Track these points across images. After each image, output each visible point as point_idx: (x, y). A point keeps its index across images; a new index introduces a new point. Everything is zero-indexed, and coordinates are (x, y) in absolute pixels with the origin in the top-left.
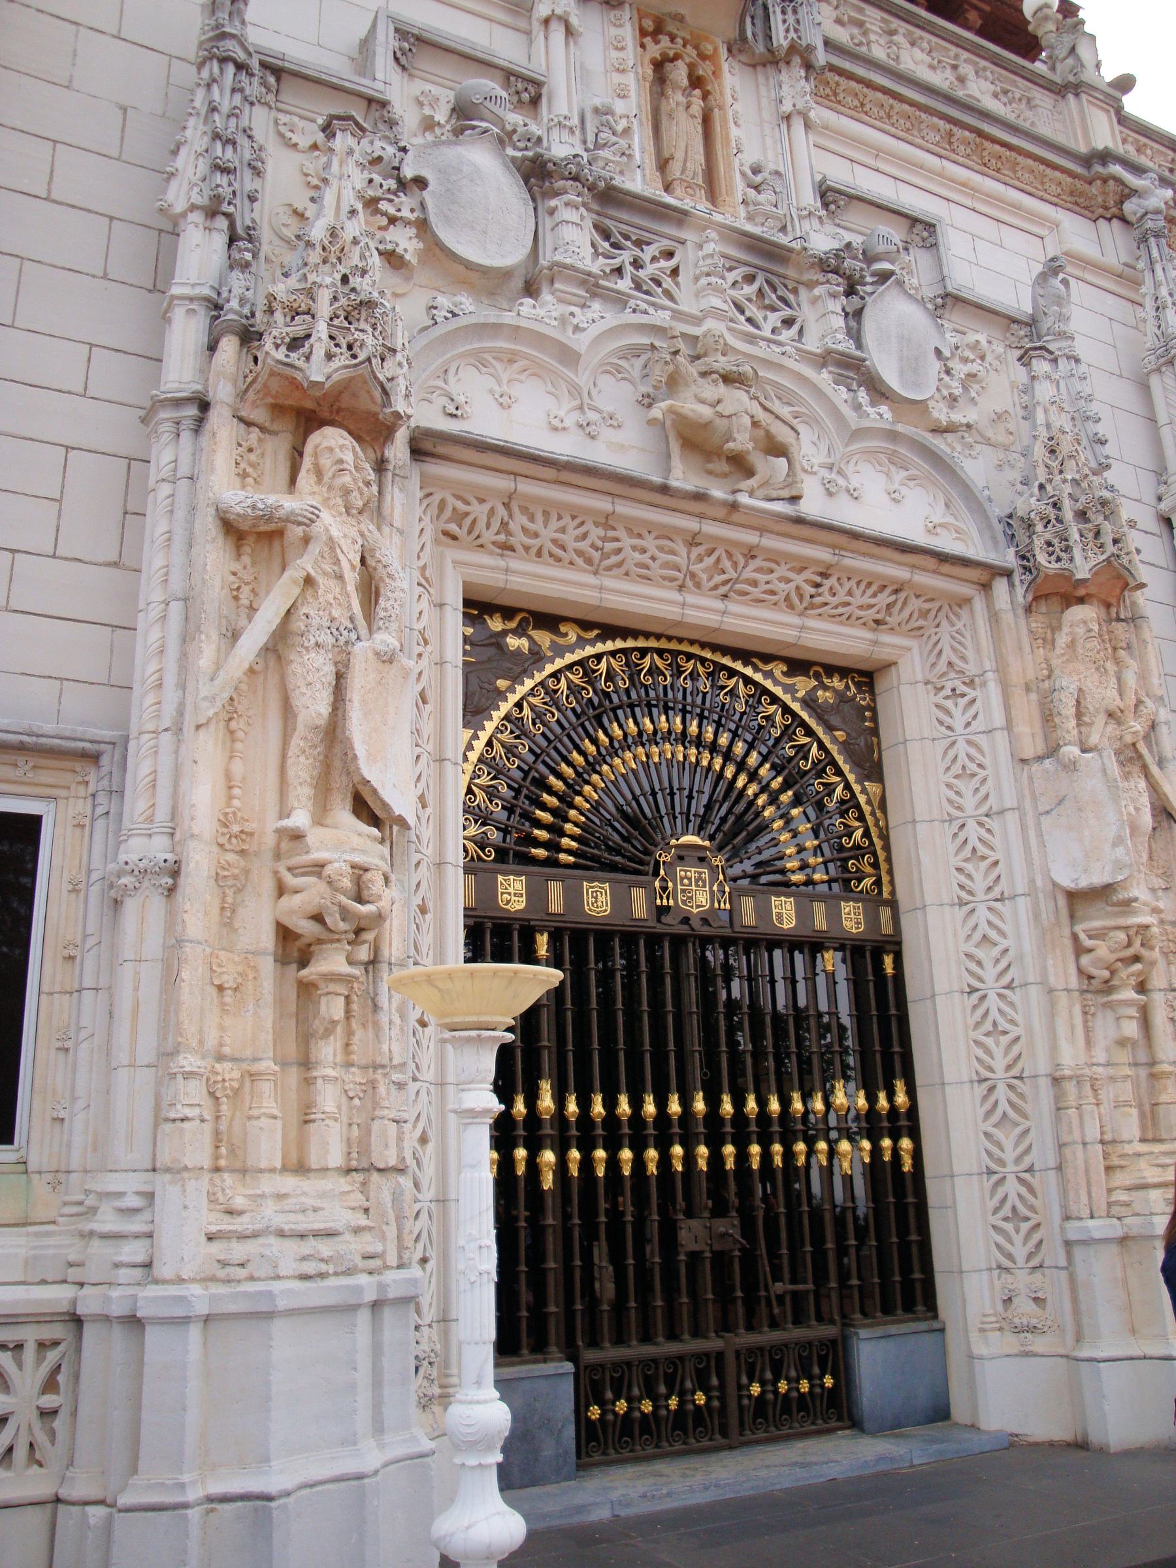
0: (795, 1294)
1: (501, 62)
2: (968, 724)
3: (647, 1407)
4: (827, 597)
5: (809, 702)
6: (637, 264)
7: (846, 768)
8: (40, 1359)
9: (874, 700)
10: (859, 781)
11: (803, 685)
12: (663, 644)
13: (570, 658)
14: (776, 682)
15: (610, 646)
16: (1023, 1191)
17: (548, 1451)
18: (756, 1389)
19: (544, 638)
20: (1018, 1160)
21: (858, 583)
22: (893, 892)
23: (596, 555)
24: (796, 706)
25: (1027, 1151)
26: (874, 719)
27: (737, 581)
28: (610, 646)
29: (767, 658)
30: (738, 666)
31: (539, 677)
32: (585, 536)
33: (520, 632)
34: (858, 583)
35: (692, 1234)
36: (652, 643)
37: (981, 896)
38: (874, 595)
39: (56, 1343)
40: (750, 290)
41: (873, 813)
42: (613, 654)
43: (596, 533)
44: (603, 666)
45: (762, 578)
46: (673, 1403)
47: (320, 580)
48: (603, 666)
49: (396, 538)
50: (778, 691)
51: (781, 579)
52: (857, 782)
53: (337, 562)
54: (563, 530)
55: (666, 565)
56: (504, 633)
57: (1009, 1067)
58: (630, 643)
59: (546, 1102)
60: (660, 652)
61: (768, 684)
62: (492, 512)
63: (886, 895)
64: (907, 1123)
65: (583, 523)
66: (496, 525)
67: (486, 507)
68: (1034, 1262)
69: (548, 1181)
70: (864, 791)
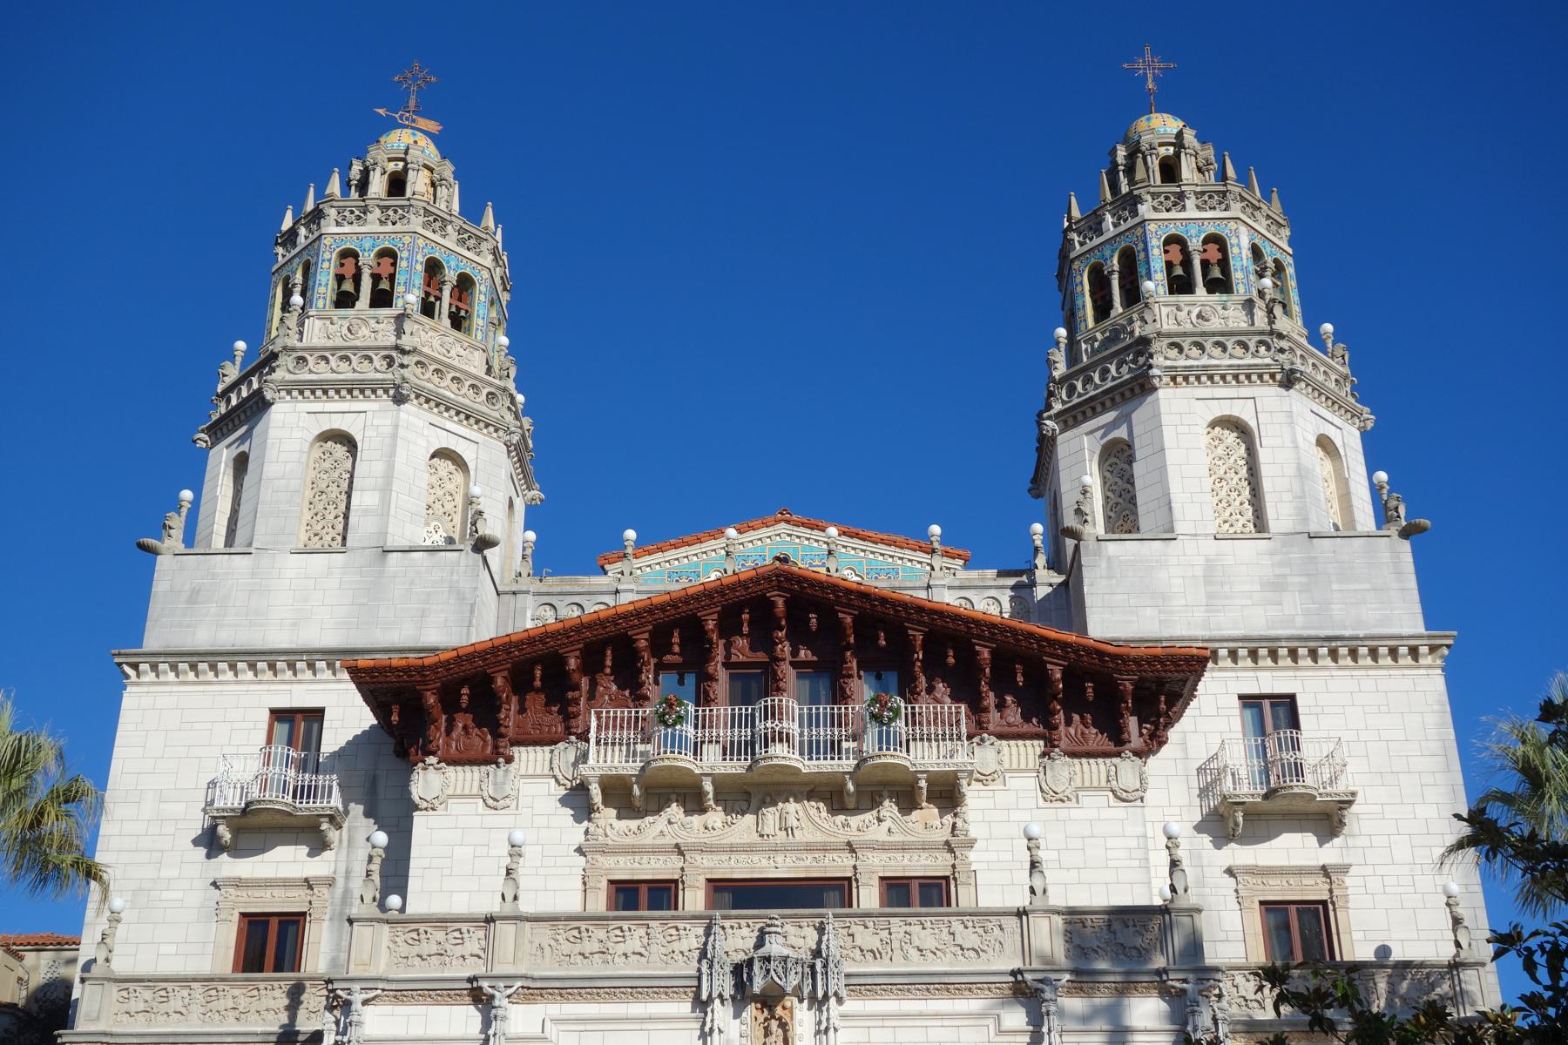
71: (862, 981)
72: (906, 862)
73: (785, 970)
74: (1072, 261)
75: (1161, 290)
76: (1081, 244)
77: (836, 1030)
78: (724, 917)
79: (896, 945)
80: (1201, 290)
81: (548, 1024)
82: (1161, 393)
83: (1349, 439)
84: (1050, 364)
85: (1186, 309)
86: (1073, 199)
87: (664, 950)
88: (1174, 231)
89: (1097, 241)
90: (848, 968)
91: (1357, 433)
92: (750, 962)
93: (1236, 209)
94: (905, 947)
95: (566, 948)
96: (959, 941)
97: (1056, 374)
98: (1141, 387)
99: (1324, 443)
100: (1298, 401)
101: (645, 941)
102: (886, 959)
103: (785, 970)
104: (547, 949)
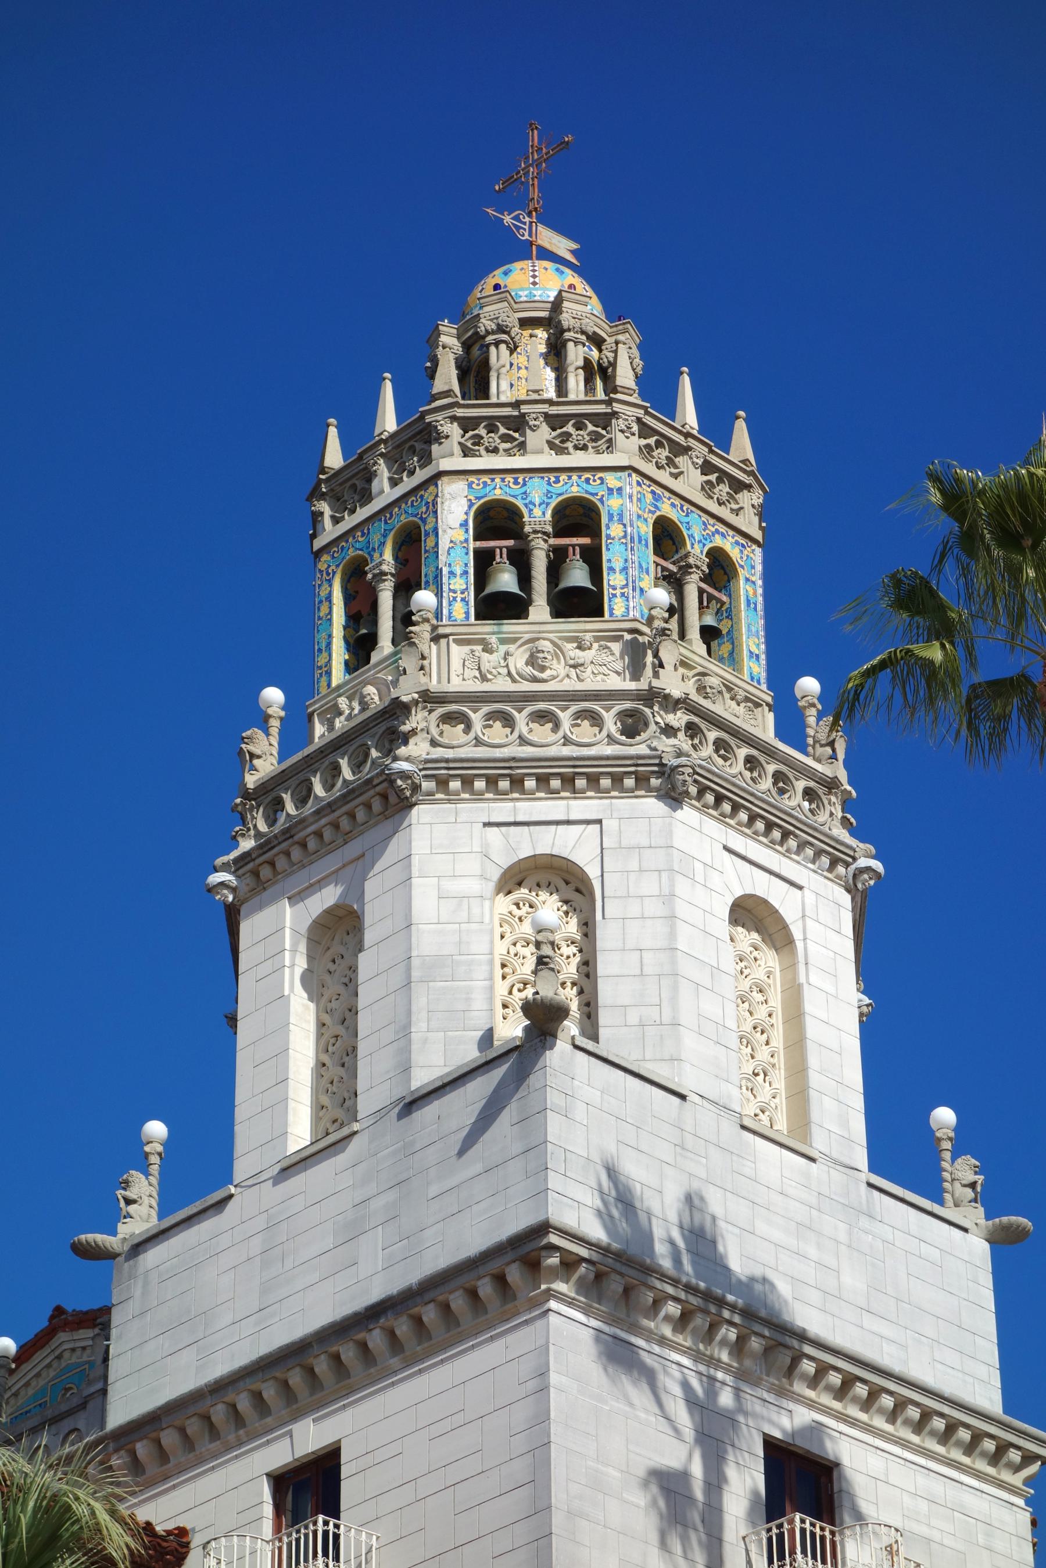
74: (318, 554)
75: (459, 611)
76: (336, 521)
80: (540, 610)
82: (421, 814)
83: (823, 916)
84: (245, 760)
85: (503, 648)
86: (333, 432)
88: (498, 494)
89: (363, 513)
91: (846, 899)
93: (627, 449)
97: (251, 780)
98: (390, 802)
99: (749, 913)
100: (695, 829)
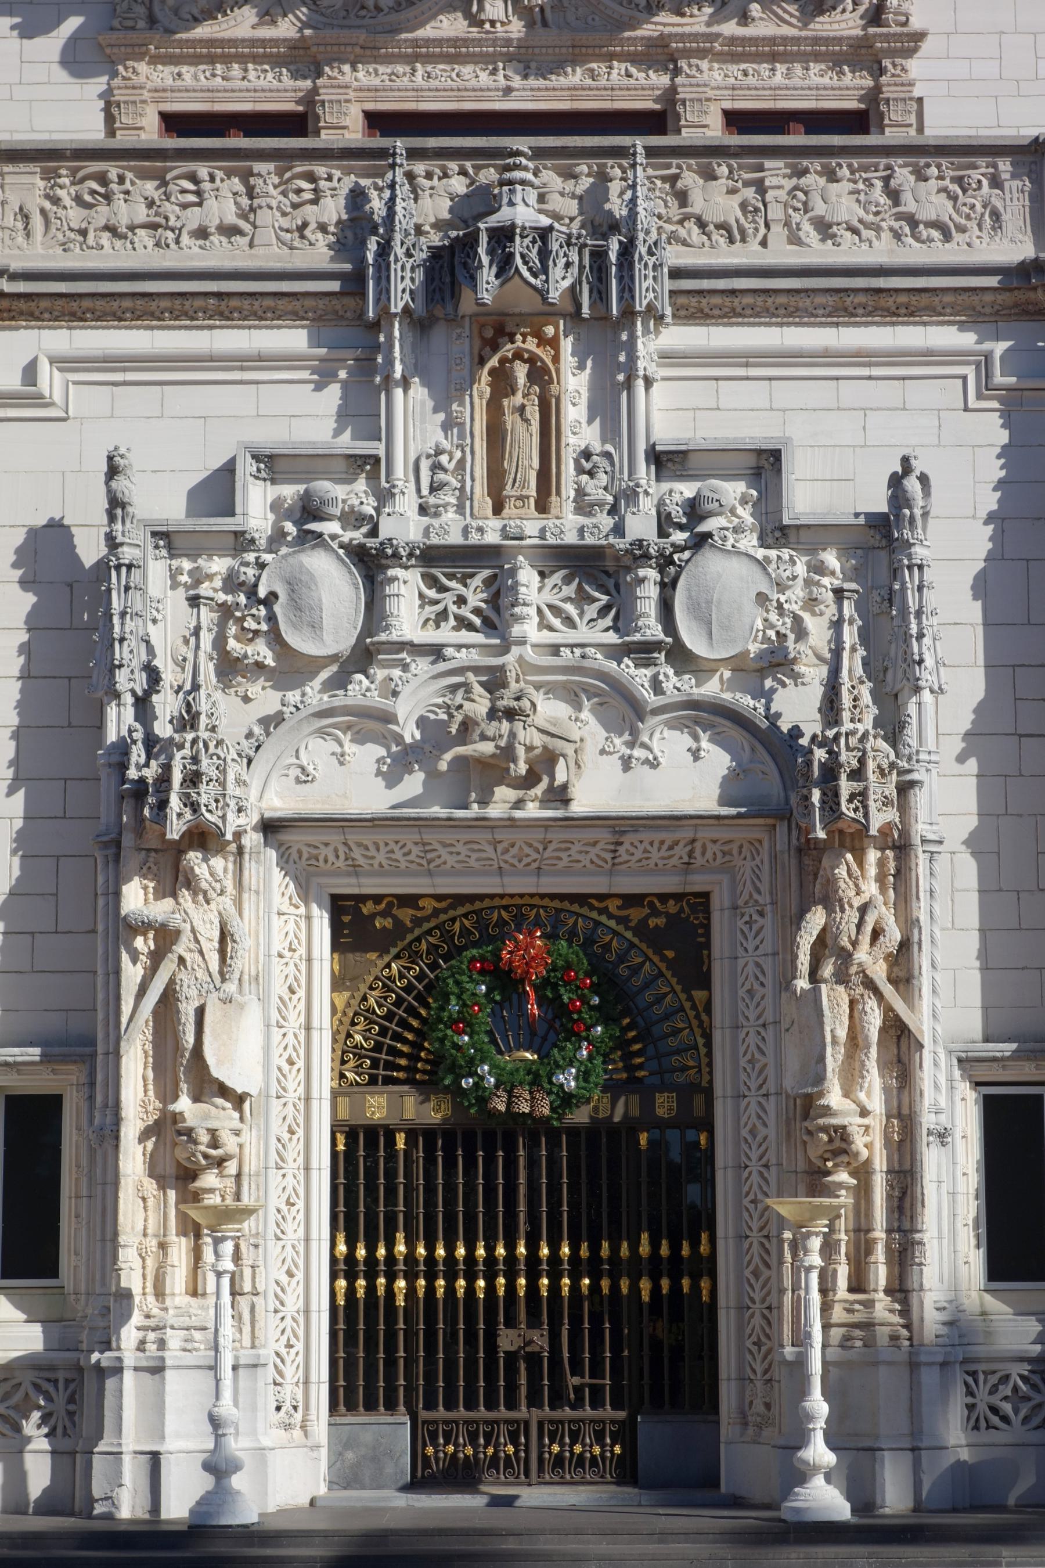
0: (592, 1387)
1: (339, 451)
2: (757, 948)
3: (469, 1451)
4: (625, 857)
5: (641, 929)
6: (461, 601)
7: (674, 981)
8: (66, 1388)
9: (708, 919)
10: (686, 990)
11: (635, 914)
12: (505, 902)
13: (426, 926)
14: (610, 916)
15: (461, 910)
16: (764, 1323)
17: (389, 1469)
18: (556, 1448)
19: (406, 915)
20: (763, 1300)
21: (651, 844)
22: (711, 1082)
23: (424, 862)
24: (629, 935)
25: (769, 1293)
26: (708, 934)
27: (542, 860)
28: (461, 910)
29: (601, 897)
30: (575, 908)
31: (401, 945)
32: (409, 853)
33: (384, 914)
34: (651, 844)
35: (508, 1340)
36: (497, 902)
37: (753, 1093)
38: (671, 848)
39: (74, 1380)
40: (570, 590)
41: (698, 1017)
42: (465, 916)
43: (416, 850)
44: (457, 925)
45: (563, 855)
46: (490, 1451)
47: (187, 956)
48: (457, 926)
49: (253, 897)
50: (612, 923)
51: (581, 852)
52: (683, 991)
53: (197, 941)
54: (392, 852)
55: (478, 860)
56: (373, 916)
57: (761, 1229)
58: (478, 905)
59: (401, 1248)
60: (506, 908)
61: (603, 919)
62: (336, 850)
63: (704, 1084)
64: (708, 1267)
65: (404, 845)
66: (342, 856)
67: (331, 848)
68: (767, 1377)
69: (400, 1302)
70: (690, 998)
71: (706, 284)
72: (778, 79)
73: (544, 254)
77: (648, 382)
78: (414, 154)
79: (775, 212)
81: (44, 368)
87: (285, 222)
90: (674, 256)
92: (469, 242)
94: (796, 217)
95: (75, 215)
96: (909, 205)
101: (245, 201)
102: (754, 245)
103: (544, 254)
104: (37, 221)
